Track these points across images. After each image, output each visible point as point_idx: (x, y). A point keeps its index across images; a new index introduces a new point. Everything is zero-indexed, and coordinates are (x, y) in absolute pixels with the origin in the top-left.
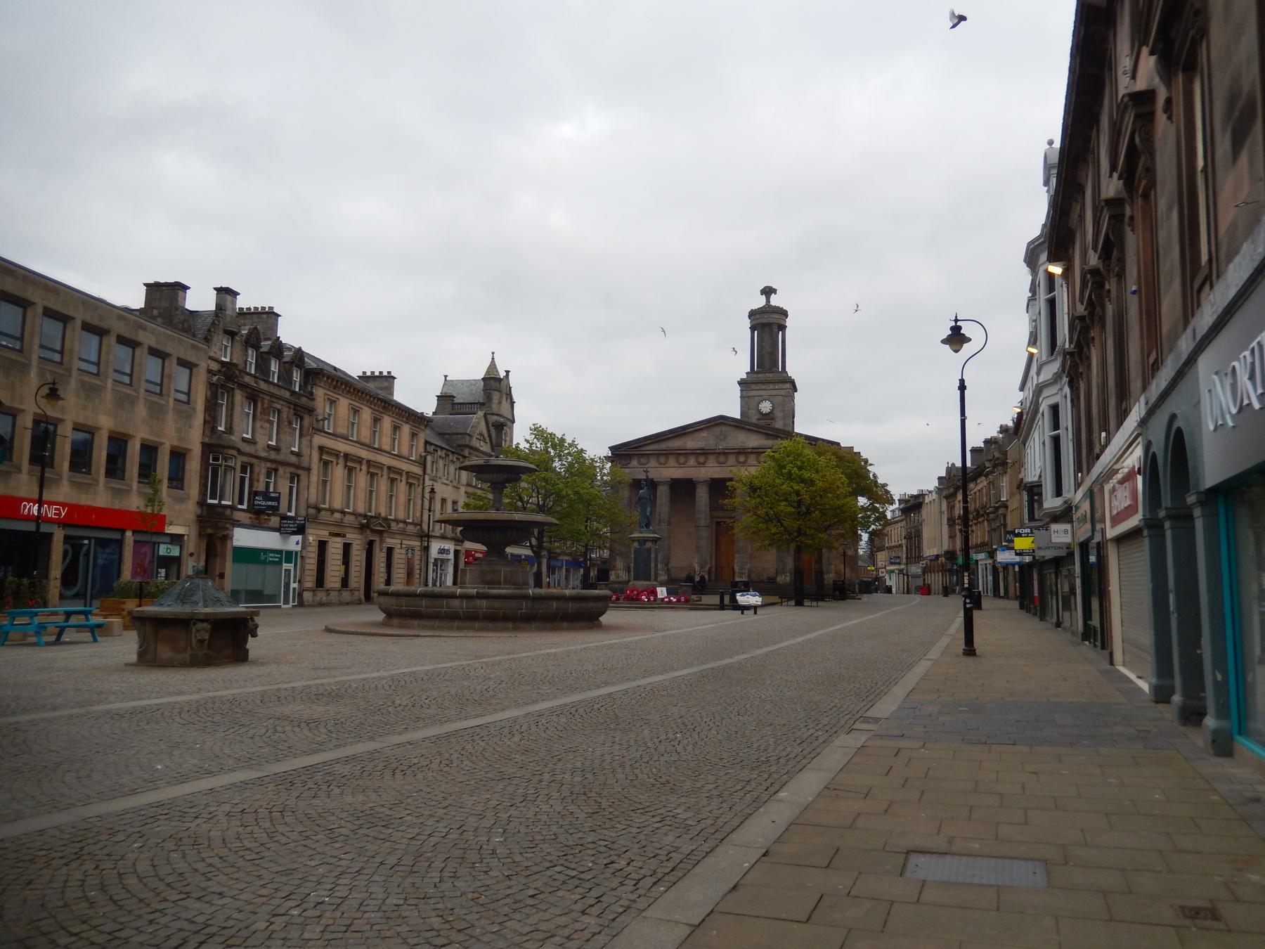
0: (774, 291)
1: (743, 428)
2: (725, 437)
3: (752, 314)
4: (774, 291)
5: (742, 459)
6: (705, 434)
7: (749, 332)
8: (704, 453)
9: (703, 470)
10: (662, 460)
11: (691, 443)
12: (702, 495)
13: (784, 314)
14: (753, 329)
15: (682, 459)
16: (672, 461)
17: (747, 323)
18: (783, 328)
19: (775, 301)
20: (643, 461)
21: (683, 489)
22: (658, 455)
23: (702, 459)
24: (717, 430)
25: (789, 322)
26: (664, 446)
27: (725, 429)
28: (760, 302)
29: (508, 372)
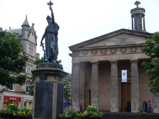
0: (139, 3)
1: (134, 35)
2: (125, 39)
3: (132, 11)
4: (139, 3)
5: (133, 50)
6: (115, 39)
7: (131, 18)
8: (115, 48)
9: (114, 56)
10: (94, 52)
11: (108, 44)
12: (114, 68)
13: (143, 10)
14: (132, 16)
15: (104, 51)
16: (99, 53)
17: (130, 15)
18: (143, 16)
19: (140, 6)
20: (85, 53)
21: (104, 66)
22: (92, 50)
23: (113, 51)
24: (121, 36)
25: (146, 14)
26: (95, 45)
27: (125, 36)
28: (135, 7)
29: (33, 24)
